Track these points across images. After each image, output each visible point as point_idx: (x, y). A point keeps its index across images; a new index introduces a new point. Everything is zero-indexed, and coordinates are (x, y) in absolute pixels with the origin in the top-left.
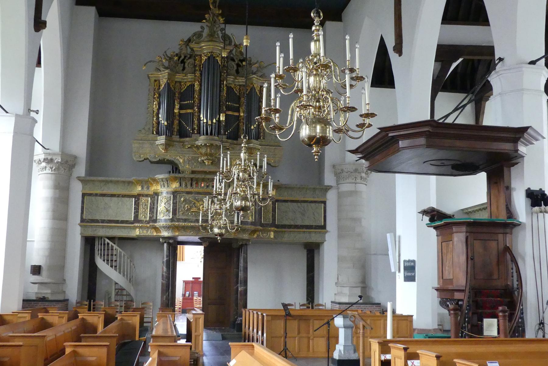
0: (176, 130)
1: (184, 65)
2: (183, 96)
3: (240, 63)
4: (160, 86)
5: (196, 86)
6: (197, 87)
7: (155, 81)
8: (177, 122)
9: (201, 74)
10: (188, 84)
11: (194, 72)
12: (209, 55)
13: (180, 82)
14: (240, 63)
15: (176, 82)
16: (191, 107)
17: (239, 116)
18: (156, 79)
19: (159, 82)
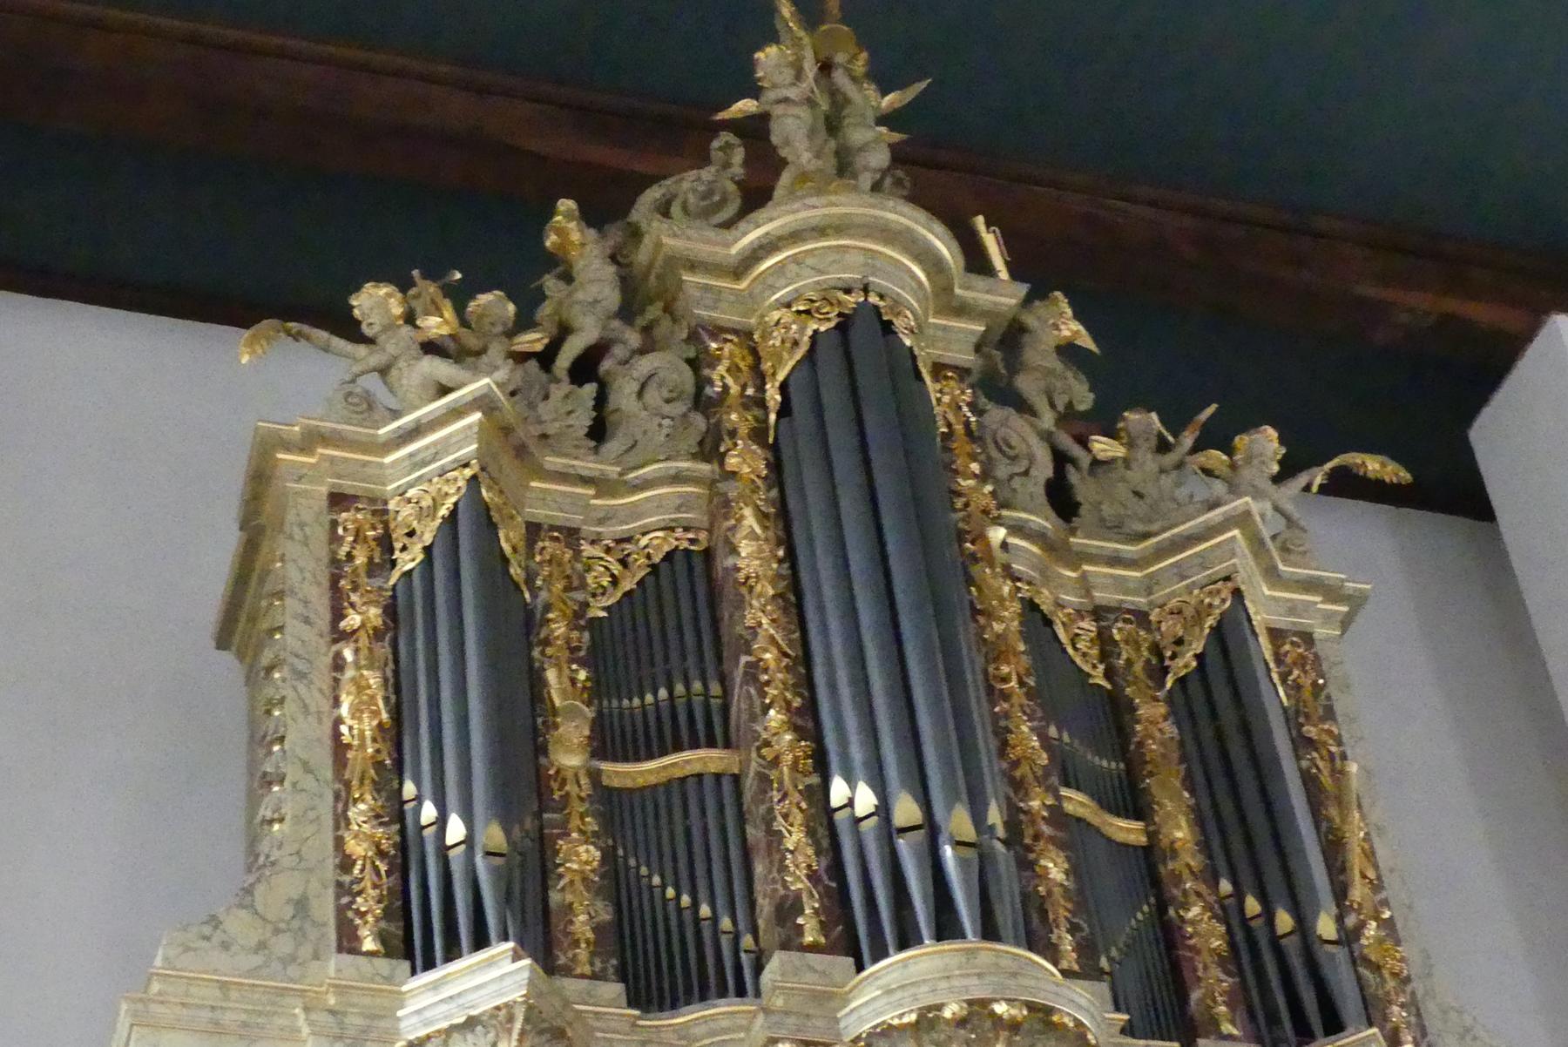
0: (581, 925)
1: (601, 400)
2: (615, 650)
3: (1066, 442)
4: (386, 543)
5: (745, 548)
6: (750, 552)
7: (339, 500)
8: (589, 854)
9: (776, 466)
10: (658, 544)
11: (710, 448)
12: (852, 300)
13: (571, 535)
14: (1066, 442)
15: (534, 530)
16: (714, 729)
17: (1150, 856)
18: (348, 486)
19: (381, 513)
